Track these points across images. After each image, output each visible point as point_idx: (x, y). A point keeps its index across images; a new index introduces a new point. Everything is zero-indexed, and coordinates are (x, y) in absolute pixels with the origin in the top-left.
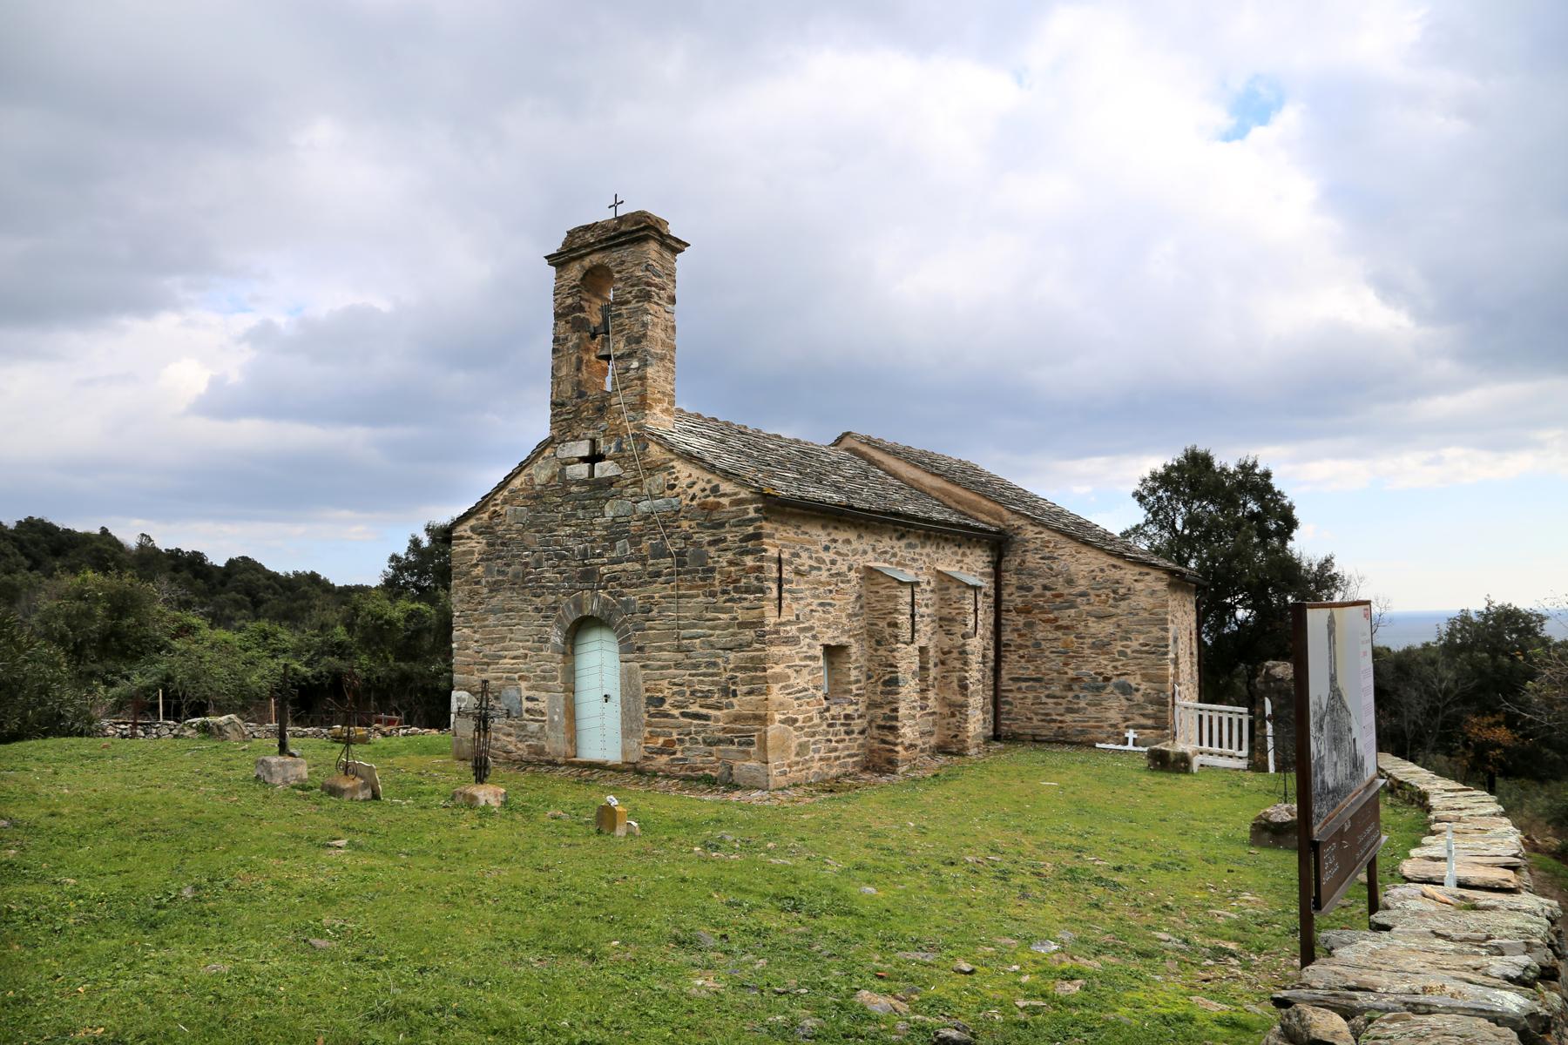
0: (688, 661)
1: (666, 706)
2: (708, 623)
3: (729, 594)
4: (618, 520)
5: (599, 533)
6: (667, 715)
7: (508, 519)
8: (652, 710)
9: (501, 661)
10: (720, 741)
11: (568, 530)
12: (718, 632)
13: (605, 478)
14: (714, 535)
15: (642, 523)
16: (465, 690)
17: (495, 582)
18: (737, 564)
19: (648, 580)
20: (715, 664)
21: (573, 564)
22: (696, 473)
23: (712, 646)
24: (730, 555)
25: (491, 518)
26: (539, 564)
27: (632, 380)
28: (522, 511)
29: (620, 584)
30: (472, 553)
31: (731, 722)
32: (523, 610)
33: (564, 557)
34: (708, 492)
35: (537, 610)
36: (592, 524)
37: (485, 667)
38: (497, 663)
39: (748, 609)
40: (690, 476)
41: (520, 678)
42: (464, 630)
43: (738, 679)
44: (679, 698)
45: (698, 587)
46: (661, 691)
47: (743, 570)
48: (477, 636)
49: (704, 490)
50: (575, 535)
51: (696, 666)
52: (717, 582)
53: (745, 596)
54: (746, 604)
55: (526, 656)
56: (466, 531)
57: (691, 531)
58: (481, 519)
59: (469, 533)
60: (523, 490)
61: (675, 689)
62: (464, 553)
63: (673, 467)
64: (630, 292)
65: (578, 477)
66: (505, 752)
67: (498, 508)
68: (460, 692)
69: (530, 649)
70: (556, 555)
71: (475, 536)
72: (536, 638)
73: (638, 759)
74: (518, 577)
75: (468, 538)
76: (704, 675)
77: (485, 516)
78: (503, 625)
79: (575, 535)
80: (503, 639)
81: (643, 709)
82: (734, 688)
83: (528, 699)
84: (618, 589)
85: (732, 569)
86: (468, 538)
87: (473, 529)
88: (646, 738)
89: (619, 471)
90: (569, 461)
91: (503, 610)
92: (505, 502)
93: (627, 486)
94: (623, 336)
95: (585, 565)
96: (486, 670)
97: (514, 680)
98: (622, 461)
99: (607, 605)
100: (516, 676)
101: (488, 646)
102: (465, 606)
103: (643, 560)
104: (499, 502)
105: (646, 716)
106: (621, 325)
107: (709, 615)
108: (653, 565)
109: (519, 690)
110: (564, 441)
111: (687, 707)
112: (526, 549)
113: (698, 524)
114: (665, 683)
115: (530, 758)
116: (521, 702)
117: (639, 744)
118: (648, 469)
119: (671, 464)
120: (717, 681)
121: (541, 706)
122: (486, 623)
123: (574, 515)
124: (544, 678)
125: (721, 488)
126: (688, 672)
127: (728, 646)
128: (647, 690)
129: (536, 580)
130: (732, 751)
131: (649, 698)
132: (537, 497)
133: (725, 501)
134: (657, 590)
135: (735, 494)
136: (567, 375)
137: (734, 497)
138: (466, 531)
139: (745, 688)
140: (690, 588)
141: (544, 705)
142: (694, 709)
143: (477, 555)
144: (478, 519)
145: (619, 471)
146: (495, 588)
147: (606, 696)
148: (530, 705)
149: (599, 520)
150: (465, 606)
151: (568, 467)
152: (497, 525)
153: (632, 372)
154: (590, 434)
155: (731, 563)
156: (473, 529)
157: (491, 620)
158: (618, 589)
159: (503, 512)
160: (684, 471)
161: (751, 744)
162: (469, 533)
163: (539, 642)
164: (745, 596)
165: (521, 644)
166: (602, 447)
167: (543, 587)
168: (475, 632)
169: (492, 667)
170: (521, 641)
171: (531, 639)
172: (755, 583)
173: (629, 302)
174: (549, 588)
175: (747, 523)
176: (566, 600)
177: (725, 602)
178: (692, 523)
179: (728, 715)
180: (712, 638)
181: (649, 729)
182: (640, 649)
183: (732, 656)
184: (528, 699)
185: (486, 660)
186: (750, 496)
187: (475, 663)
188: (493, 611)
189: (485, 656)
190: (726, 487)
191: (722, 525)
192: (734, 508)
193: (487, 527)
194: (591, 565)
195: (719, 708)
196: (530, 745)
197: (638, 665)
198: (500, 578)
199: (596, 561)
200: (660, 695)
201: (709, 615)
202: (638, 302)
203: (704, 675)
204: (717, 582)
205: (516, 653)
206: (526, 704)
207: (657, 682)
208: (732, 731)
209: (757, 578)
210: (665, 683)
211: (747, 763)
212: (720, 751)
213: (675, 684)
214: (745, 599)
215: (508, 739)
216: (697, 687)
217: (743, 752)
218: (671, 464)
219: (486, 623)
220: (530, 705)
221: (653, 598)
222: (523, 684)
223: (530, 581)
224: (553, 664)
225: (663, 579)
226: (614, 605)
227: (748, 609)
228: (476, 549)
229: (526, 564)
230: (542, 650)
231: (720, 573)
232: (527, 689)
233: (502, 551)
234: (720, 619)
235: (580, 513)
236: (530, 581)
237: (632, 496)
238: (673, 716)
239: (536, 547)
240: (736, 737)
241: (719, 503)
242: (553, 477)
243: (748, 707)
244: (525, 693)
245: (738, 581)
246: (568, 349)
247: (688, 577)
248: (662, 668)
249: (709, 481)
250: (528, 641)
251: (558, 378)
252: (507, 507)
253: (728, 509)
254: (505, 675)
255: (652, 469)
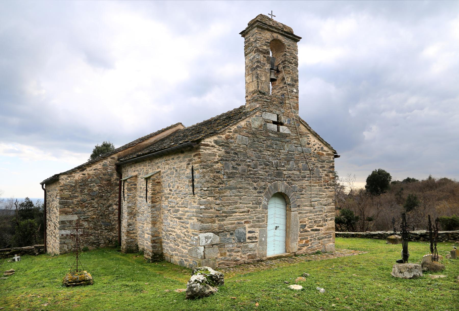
0: (314, 210)
1: (306, 228)
2: (320, 196)
3: (326, 186)
4: (290, 152)
5: (282, 156)
6: (307, 231)
7: (237, 141)
8: (302, 230)
9: (234, 215)
10: (323, 238)
11: (269, 153)
12: (323, 199)
13: (284, 134)
14: (322, 164)
15: (299, 155)
16: (210, 232)
17: (231, 173)
18: (328, 176)
19: (302, 179)
20: (322, 211)
21: (272, 168)
22: (317, 141)
23: (321, 204)
24: (326, 172)
25: (227, 138)
26: (255, 166)
27: (294, 96)
28: (245, 139)
29: (292, 179)
30: (215, 155)
31: (326, 231)
32: (248, 188)
33: (267, 165)
34: (320, 149)
35: (255, 188)
36: (279, 152)
37: (224, 218)
38: (232, 216)
39: (331, 191)
40: (314, 141)
41: (245, 222)
42: (208, 198)
43: (328, 216)
44: (311, 224)
45: (317, 183)
46: (305, 222)
47: (330, 178)
48: (218, 202)
49: (319, 148)
50: (272, 156)
51: (316, 212)
52: (322, 181)
53: (330, 187)
54: (330, 190)
55: (249, 211)
56: (211, 142)
57: (315, 162)
58: (221, 137)
59: (213, 144)
60: (246, 128)
61: (310, 221)
62: (210, 155)
63: (309, 136)
64: (292, 60)
65: (273, 130)
66: (235, 261)
67: (231, 134)
68: (206, 234)
69: (251, 208)
70: (265, 164)
71: (217, 146)
72: (254, 202)
73: (296, 250)
74: (245, 172)
75: (212, 146)
76: (319, 215)
77: (223, 136)
78: (236, 196)
79: (272, 156)
80: (236, 203)
81: (299, 230)
82: (326, 219)
83: (250, 232)
84: (291, 181)
85: (326, 177)
86: (212, 146)
87: (216, 142)
88: (299, 241)
89: (290, 132)
90: (269, 121)
91: (236, 188)
92: (236, 132)
93: (293, 139)
94: (290, 76)
95: (278, 170)
96: (224, 220)
97: (242, 223)
98: (291, 128)
99: (287, 188)
100: (243, 222)
101: (227, 207)
102: (210, 185)
103: (299, 170)
104: (232, 131)
105: (299, 232)
106: (289, 71)
107: (321, 193)
108: (303, 173)
109: (245, 228)
110: (265, 111)
111: (313, 227)
112: (248, 158)
113: (317, 160)
114: (306, 219)
115: (249, 261)
116: (245, 234)
117: (297, 244)
118: (300, 134)
119: (308, 135)
120: (322, 217)
121: (256, 235)
122: (225, 194)
123: (271, 146)
124: (259, 221)
125: (324, 148)
126: (314, 214)
127: (325, 204)
128: (300, 222)
129: (254, 174)
130: (326, 240)
131: (302, 225)
132: (253, 134)
133: (325, 153)
134: (305, 183)
135: (328, 151)
136: (265, 81)
137: (327, 152)
138: (211, 142)
139: (329, 219)
140: (315, 183)
141: (258, 234)
142: (315, 227)
143: (218, 157)
144: (219, 137)
145: (290, 132)
146: (231, 176)
147: (276, 227)
148: (250, 235)
149: (283, 151)
150: (210, 185)
151: (268, 124)
152: (231, 143)
153: (294, 93)
154: (278, 112)
155: (326, 175)
156: (216, 142)
157: (228, 193)
158: (291, 181)
159: (235, 136)
160: (313, 139)
161: (330, 237)
162: (213, 144)
163: (256, 204)
164: (330, 187)
165: (246, 205)
166: (283, 119)
167: (259, 178)
168: (216, 199)
169: (228, 218)
170: (246, 204)
171: (251, 203)
172: (332, 183)
173: (292, 64)
174: (261, 179)
175: (331, 162)
176: (269, 185)
177: (325, 189)
178: (315, 159)
179: (325, 228)
180: (320, 201)
181: (300, 238)
182: (299, 206)
183: (326, 207)
184: (250, 232)
185: (224, 214)
186: (332, 153)
187: (217, 216)
188: (230, 188)
189: (223, 212)
190: (325, 148)
191: (324, 161)
192: (327, 156)
193: (226, 143)
194: (280, 170)
195: (322, 226)
196: (249, 255)
197: (297, 212)
198: (235, 171)
199: (282, 168)
200: (305, 224)
201: (321, 193)
202: (295, 65)
203: (319, 215)
204: (322, 181)
205: (243, 210)
206: (248, 235)
207: (304, 219)
208: (326, 234)
209: (333, 181)
210: (306, 219)
211: (330, 244)
212: (323, 241)
213: (310, 219)
214: (330, 188)
215: (237, 254)
216: (316, 219)
217: (329, 240)
218: (308, 135)
219: (225, 194)
220: (250, 235)
221: (303, 186)
222: (247, 225)
223: (251, 174)
224: (263, 214)
225: (306, 179)
226: (290, 188)
227: (331, 191)
228: (217, 154)
229: (249, 166)
230: (257, 208)
231: (323, 178)
232: (249, 227)
233: (235, 157)
234: (323, 195)
235: (275, 146)
236: (251, 174)
237: (295, 144)
238: (308, 231)
239: (254, 158)
240: (327, 235)
241: (323, 154)
242: (261, 126)
243: (330, 225)
244: (248, 230)
245: (328, 182)
246: (265, 69)
247: (315, 179)
248: (306, 213)
249: (320, 145)
250: (250, 204)
251: (261, 80)
252: (237, 135)
253: (325, 156)
254: (236, 222)
255: (302, 135)
